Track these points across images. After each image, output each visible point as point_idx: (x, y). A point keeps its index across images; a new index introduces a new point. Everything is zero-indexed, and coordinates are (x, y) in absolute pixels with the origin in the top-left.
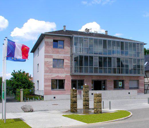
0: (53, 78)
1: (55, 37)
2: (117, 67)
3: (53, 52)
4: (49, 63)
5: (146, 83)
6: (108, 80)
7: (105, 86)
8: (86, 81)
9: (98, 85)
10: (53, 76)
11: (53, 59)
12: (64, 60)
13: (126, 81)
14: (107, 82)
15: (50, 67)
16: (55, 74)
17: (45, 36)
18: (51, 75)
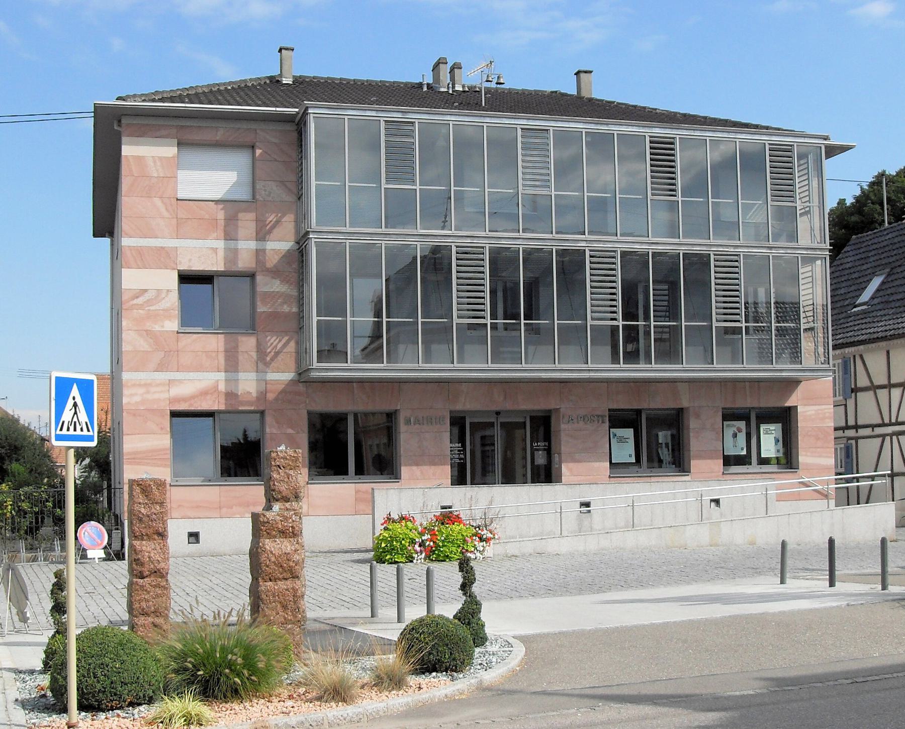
0: (184, 400)
1: (188, 123)
2: (494, 316)
3: (178, 225)
4: (149, 302)
5: (867, 432)
6: (565, 407)
7: (549, 451)
8: (408, 422)
9: (508, 444)
10: (176, 391)
11: (186, 278)
12: (259, 278)
13: (698, 416)
14: (563, 426)
15: (157, 328)
16: (192, 375)
17: (124, 121)
18: (171, 382)
